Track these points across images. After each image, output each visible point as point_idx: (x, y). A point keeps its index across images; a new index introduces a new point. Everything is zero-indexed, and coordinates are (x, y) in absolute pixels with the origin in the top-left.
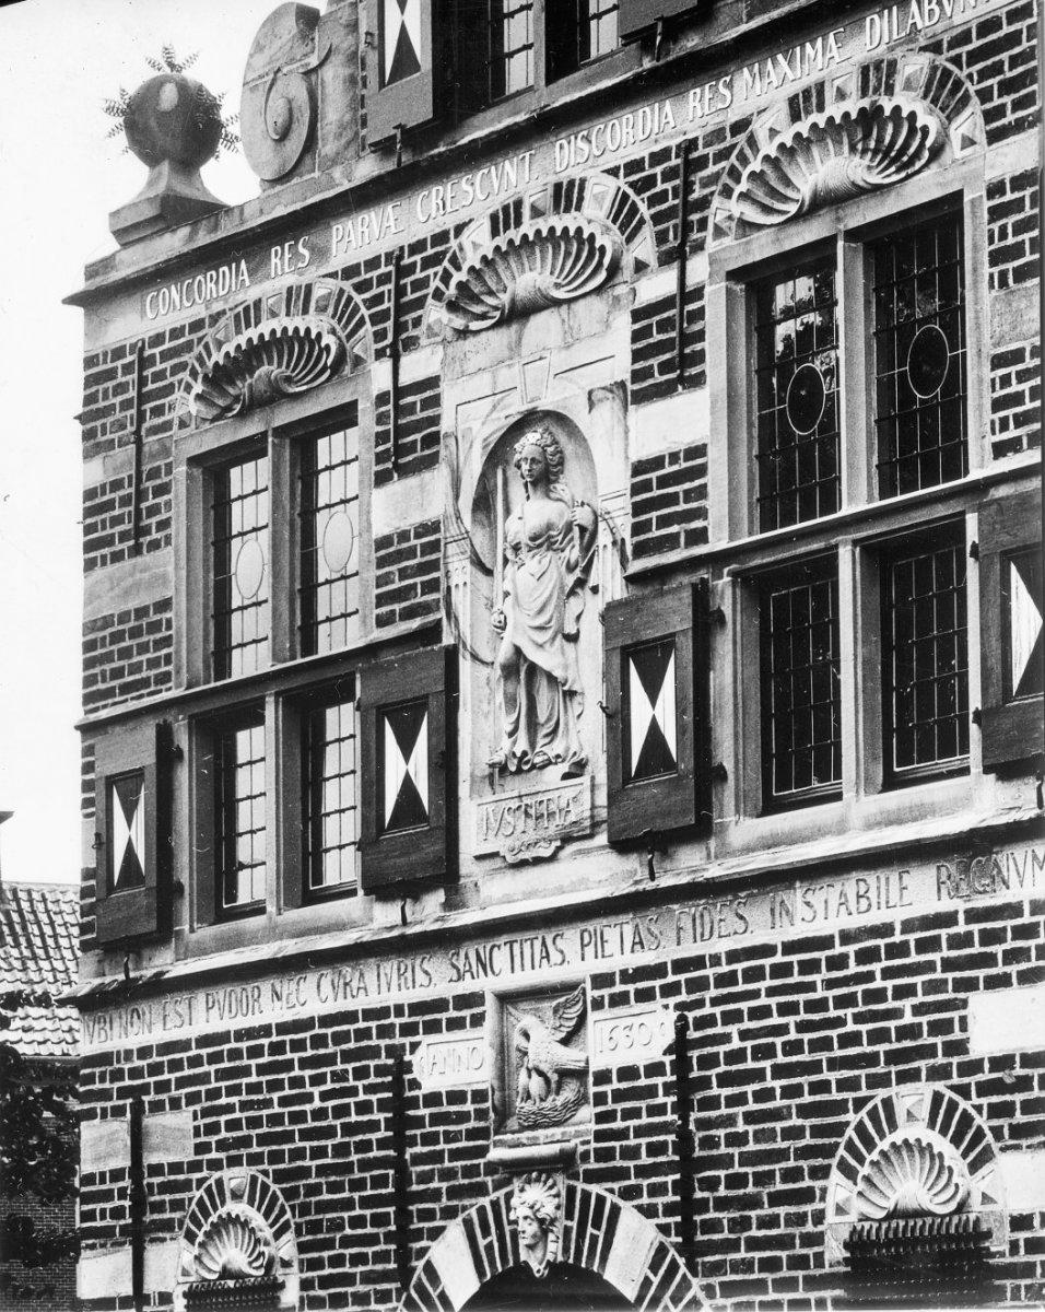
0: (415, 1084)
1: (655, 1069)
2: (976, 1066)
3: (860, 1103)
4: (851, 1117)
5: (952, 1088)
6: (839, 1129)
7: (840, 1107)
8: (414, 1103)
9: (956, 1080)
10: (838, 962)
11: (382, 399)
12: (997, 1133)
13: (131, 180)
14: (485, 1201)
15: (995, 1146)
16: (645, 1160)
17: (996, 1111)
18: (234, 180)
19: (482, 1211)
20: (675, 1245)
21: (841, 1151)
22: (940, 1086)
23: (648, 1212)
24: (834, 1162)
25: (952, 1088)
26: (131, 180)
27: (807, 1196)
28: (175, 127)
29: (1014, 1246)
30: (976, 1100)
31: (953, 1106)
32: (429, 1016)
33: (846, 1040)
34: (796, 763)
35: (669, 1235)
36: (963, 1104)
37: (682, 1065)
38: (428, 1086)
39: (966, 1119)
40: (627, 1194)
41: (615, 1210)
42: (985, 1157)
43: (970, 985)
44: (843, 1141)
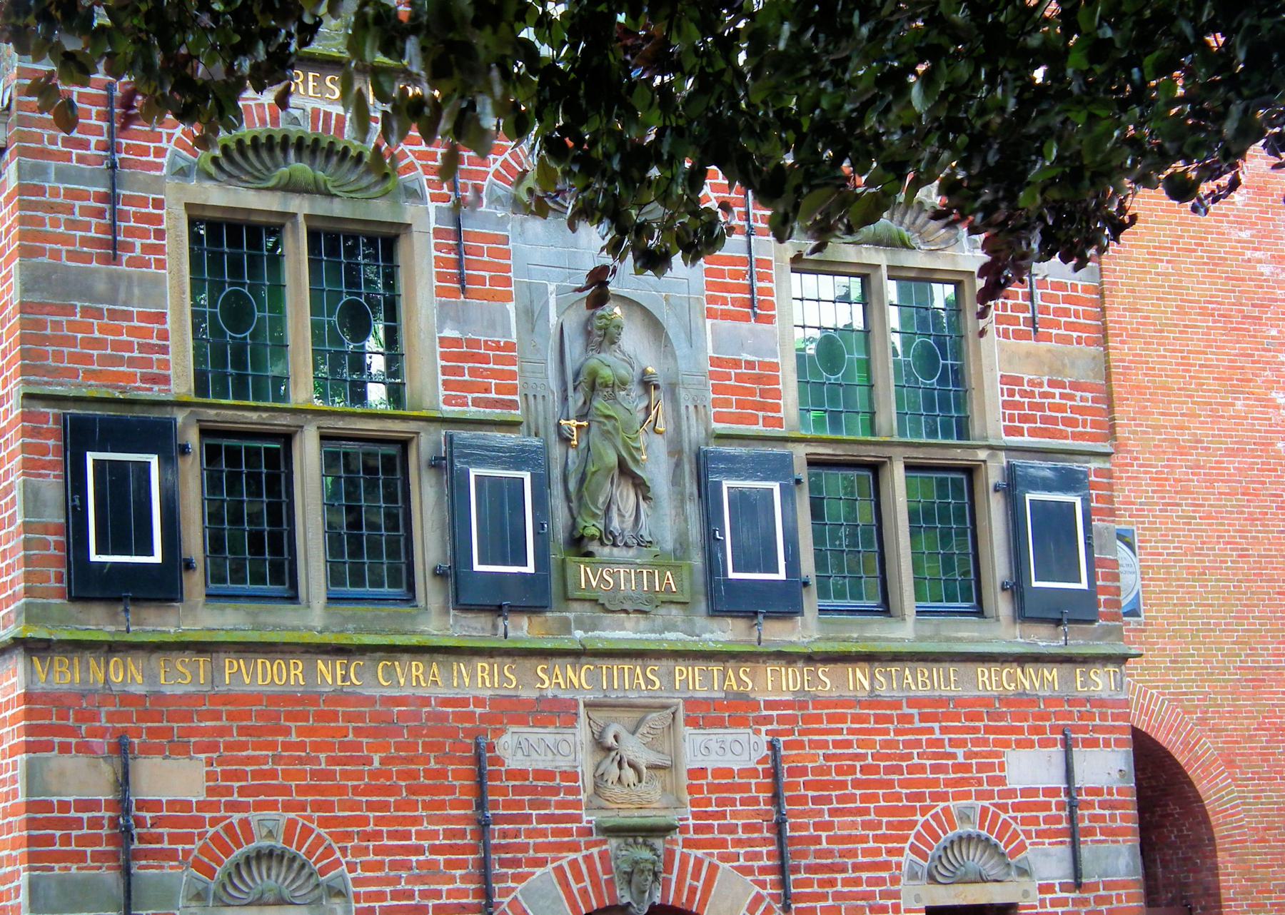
0: (498, 761)
1: (753, 773)
2: (1011, 793)
3: (924, 810)
4: (919, 818)
5: (994, 805)
6: (912, 824)
7: (912, 810)
8: (496, 776)
9: (996, 800)
10: (907, 718)
11: (438, 233)
12: (1028, 834)
14: (579, 856)
15: (1027, 842)
16: (741, 835)
17: (1024, 821)
19: (573, 864)
20: (771, 895)
21: (912, 839)
22: (986, 803)
23: (746, 871)
24: (907, 846)
25: (994, 805)
27: (885, 866)
29: (1042, 901)
30: (1012, 814)
31: (996, 816)
32: (511, 711)
33: (912, 769)
35: (765, 888)
36: (1003, 816)
37: (774, 773)
38: (514, 762)
39: (1006, 824)
40: (724, 858)
41: (713, 869)
42: (1022, 847)
43: (1006, 744)
44: (913, 833)
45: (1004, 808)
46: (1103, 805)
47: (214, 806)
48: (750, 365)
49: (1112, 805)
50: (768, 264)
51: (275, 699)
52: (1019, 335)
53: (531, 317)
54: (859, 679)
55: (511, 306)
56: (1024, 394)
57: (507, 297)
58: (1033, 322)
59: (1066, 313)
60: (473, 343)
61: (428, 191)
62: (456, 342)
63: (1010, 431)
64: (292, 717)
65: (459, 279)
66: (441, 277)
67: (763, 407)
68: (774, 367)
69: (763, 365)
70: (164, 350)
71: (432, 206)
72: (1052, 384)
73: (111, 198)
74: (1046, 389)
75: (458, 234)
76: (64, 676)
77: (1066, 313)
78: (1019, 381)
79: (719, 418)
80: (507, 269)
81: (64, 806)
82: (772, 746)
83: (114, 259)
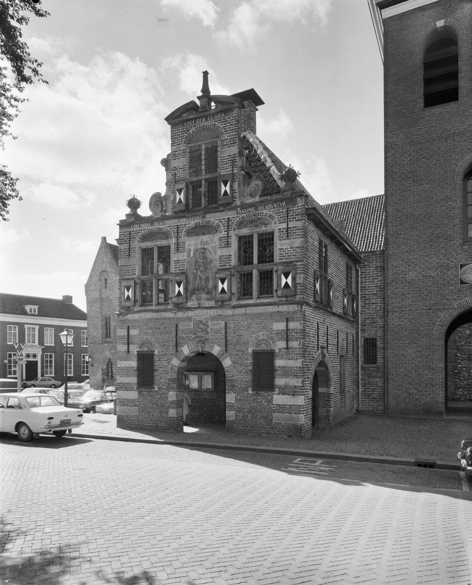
6: (252, 337)
11: (175, 243)
13: (128, 210)
18: (145, 211)
26: (128, 210)
28: (134, 204)
31: (270, 335)
34: (245, 292)
45: (272, 334)
46: (295, 333)
47: (139, 335)
48: (226, 255)
49: (297, 333)
50: (231, 236)
51: (148, 319)
52: (283, 240)
53: (189, 255)
54: (243, 310)
55: (185, 253)
56: (283, 251)
57: (185, 252)
58: (287, 236)
59: (296, 233)
60: (179, 260)
61: (173, 237)
62: (176, 261)
63: (279, 260)
64: (150, 322)
65: (178, 250)
66: (174, 250)
67: (227, 263)
68: (231, 255)
69: (229, 255)
70: (135, 270)
71: (174, 239)
72: (291, 248)
73: (130, 248)
74: (289, 249)
75: (178, 243)
76: (122, 318)
77: (296, 233)
78: (283, 249)
79: (220, 266)
80: (185, 247)
81: (121, 336)
82: (226, 323)
83: (129, 257)
